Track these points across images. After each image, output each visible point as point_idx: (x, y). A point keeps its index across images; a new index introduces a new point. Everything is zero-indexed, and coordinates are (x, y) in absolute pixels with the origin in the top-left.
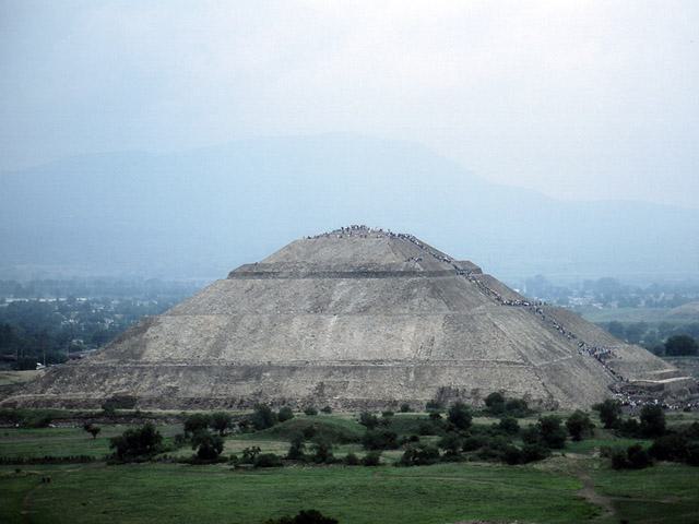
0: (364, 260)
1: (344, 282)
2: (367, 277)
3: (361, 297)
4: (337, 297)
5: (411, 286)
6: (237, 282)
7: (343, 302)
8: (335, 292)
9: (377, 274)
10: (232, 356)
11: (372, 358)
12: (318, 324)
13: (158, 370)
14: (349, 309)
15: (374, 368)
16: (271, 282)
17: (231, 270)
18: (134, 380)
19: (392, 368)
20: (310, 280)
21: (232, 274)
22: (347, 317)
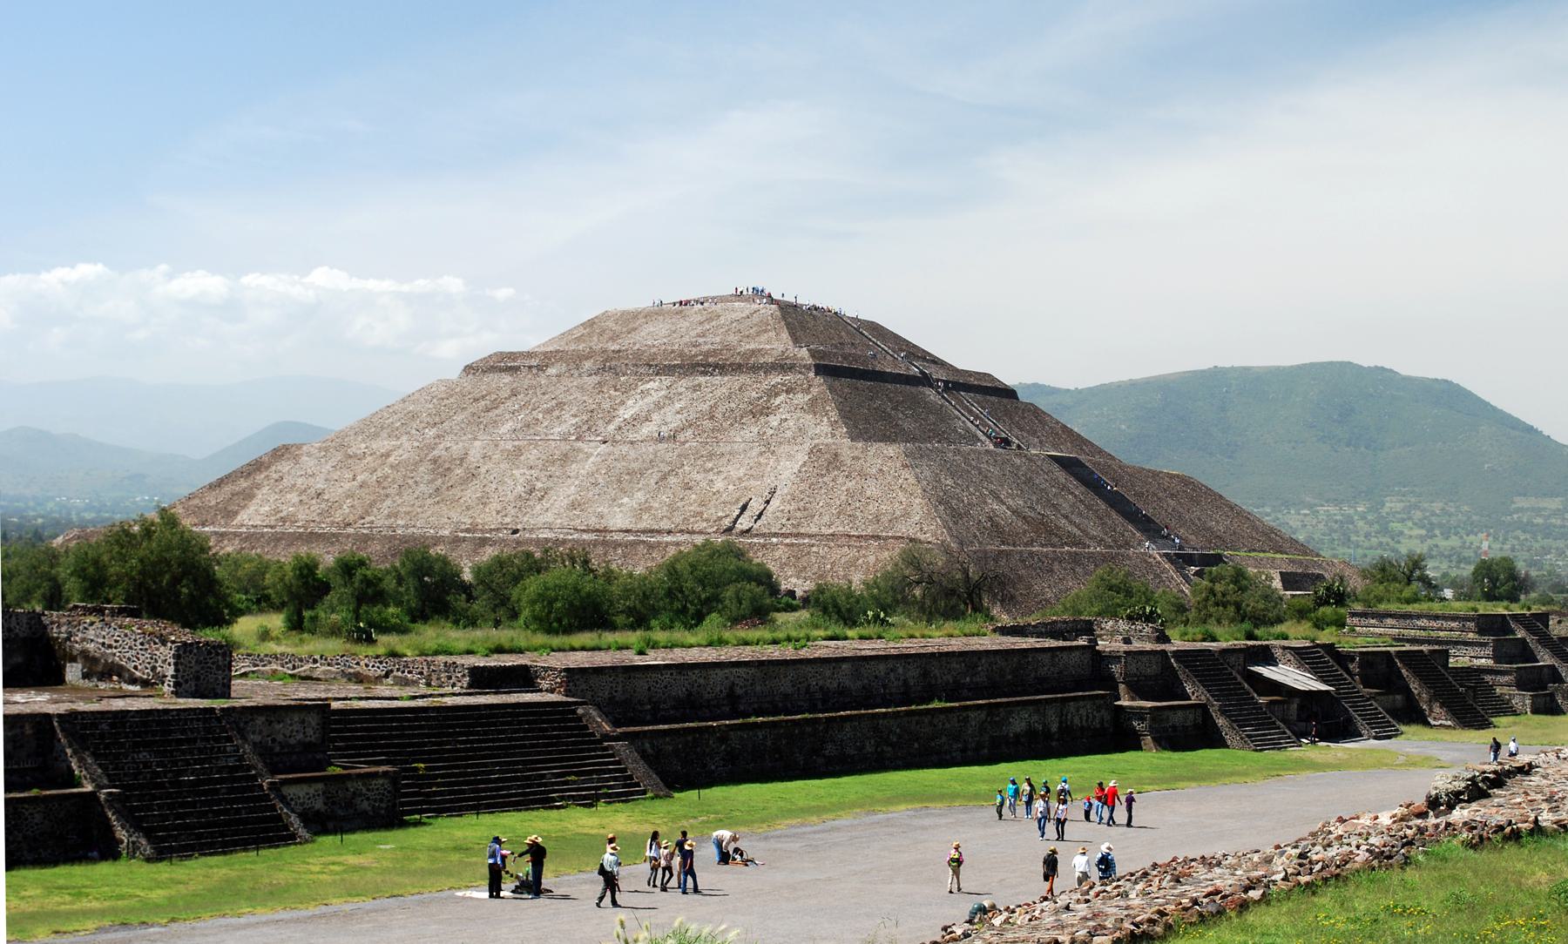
0: (712, 342)
1: (656, 387)
2: (704, 373)
3: (672, 418)
4: (626, 413)
5: (773, 392)
7: (636, 421)
8: (630, 402)
9: (722, 369)
10: (389, 516)
11: (641, 526)
12: (565, 459)
13: (252, 538)
15: (634, 544)
16: (525, 379)
19: (667, 544)
20: (596, 379)
21: (469, 369)
22: (625, 448)
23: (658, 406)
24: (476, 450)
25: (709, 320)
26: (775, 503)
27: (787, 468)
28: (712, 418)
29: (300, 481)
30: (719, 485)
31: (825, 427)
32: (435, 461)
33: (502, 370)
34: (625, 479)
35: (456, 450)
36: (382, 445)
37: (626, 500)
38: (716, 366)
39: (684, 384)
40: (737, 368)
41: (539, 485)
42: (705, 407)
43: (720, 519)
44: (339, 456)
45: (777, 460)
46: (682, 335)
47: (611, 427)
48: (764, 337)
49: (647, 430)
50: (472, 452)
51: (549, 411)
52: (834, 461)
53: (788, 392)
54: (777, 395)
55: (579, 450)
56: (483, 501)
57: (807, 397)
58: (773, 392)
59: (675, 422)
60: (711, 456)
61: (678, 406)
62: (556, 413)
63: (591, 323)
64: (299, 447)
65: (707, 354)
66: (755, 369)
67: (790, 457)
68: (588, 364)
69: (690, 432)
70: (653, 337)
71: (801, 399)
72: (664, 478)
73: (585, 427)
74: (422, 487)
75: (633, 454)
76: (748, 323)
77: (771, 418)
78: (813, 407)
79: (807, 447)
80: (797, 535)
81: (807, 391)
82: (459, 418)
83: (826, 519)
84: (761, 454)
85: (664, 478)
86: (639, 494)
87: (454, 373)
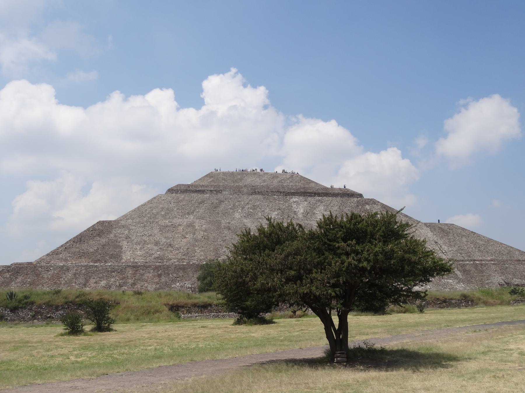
16: (220, 196)
18: (130, 281)
21: (171, 191)
29: (144, 238)
38: (315, 194)
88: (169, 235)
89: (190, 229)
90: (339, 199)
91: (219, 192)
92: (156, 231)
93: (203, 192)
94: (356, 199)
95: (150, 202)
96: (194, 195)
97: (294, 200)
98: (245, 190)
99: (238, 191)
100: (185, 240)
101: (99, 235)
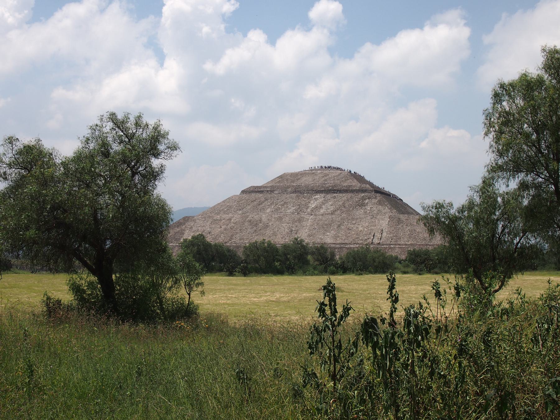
0: (330, 184)
2: (334, 193)
3: (329, 206)
4: (313, 205)
5: (363, 199)
6: (245, 196)
7: (317, 208)
9: (340, 191)
10: (240, 239)
11: (338, 242)
12: (300, 220)
14: (322, 211)
15: (341, 248)
16: (269, 196)
17: (243, 189)
20: (294, 195)
21: (243, 192)
22: (321, 217)
23: (323, 204)
24: (264, 217)
25: (326, 176)
26: (385, 234)
27: (384, 223)
28: (345, 207)
29: (200, 228)
30: (360, 229)
31: (387, 210)
32: (250, 221)
33: (256, 192)
34: (326, 227)
35: (257, 217)
36: (227, 216)
37: (328, 234)
38: (338, 190)
39: (329, 196)
40: (346, 191)
41: (294, 229)
42: (341, 203)
43: (366, 240)
44: (210, 220)
45: (379, 220)
46: (318, 181)
47: (309, 210)
48: (348, 181)
49: (322, 211)
50: (263, 219)
51: (283, 205)
52: (399, 221)
53: (369, 198)
54: (365, 200)
55: (303, 218)
56: (275, 234)
57: (377, 201)
58: (363, 199)
59: (332, 208)
60: (353, 219)
61: (330, 203)
62: (285, 206)
63: (281, 177)
64: (193, 217)
65: (332, 186)
66: (352, 191)
67: (383, 220)
68: (289, 190)
69: (339, 212)
70: (307, 181)
71: (374, 201)
72: (339, 226)
73: (299, 210)
74: (249, 230)
75: (324, 219)
76: (340, 177)
77: (366, 207)
78: (380, 203)
79: (387, 215)
80: (399, 245)
81: (376, 198)
82: (249, 207)
83: (406, 239)
84: (372, 218)
85: (339, 226)
86: (332, 232)
87: (238, 193)
88: (213, 226)
89: (228, 222)
90: (349, 195)
91: (272, 191)
92: (208, 223)
93: (261, 192)
94: (364, 194)
95: (224, 202)
96: (253, 195)
97: (316, 197)
98: (289, 190)
99: (284, 190)
100: (219, 230)
101: (178, 227)
